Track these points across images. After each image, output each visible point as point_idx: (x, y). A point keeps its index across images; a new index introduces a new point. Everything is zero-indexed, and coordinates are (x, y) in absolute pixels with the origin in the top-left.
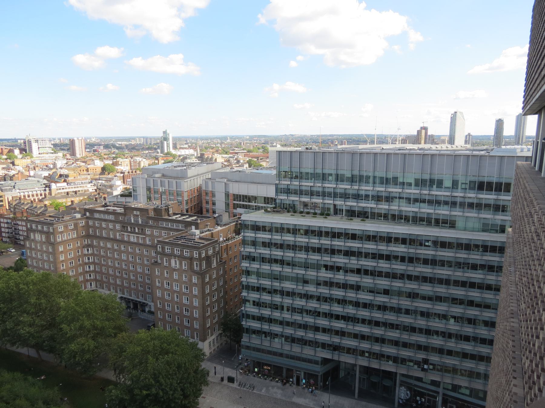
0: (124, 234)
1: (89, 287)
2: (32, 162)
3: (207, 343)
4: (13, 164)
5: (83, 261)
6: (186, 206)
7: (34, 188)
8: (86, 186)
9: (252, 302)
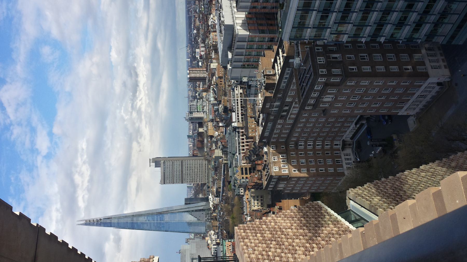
0: (289, 117)
1: (338, 146)
2: (212, 121)
3: (431, 72)
4: (212, 137)
5: (311, 150)
6: (267, 34)
7: (236, 140)
8: (237, 94)
9: (396, 31)
